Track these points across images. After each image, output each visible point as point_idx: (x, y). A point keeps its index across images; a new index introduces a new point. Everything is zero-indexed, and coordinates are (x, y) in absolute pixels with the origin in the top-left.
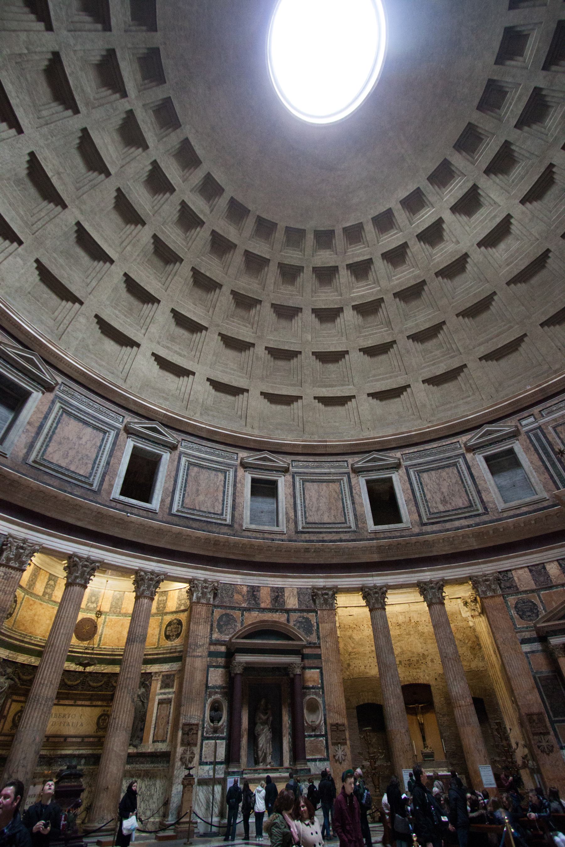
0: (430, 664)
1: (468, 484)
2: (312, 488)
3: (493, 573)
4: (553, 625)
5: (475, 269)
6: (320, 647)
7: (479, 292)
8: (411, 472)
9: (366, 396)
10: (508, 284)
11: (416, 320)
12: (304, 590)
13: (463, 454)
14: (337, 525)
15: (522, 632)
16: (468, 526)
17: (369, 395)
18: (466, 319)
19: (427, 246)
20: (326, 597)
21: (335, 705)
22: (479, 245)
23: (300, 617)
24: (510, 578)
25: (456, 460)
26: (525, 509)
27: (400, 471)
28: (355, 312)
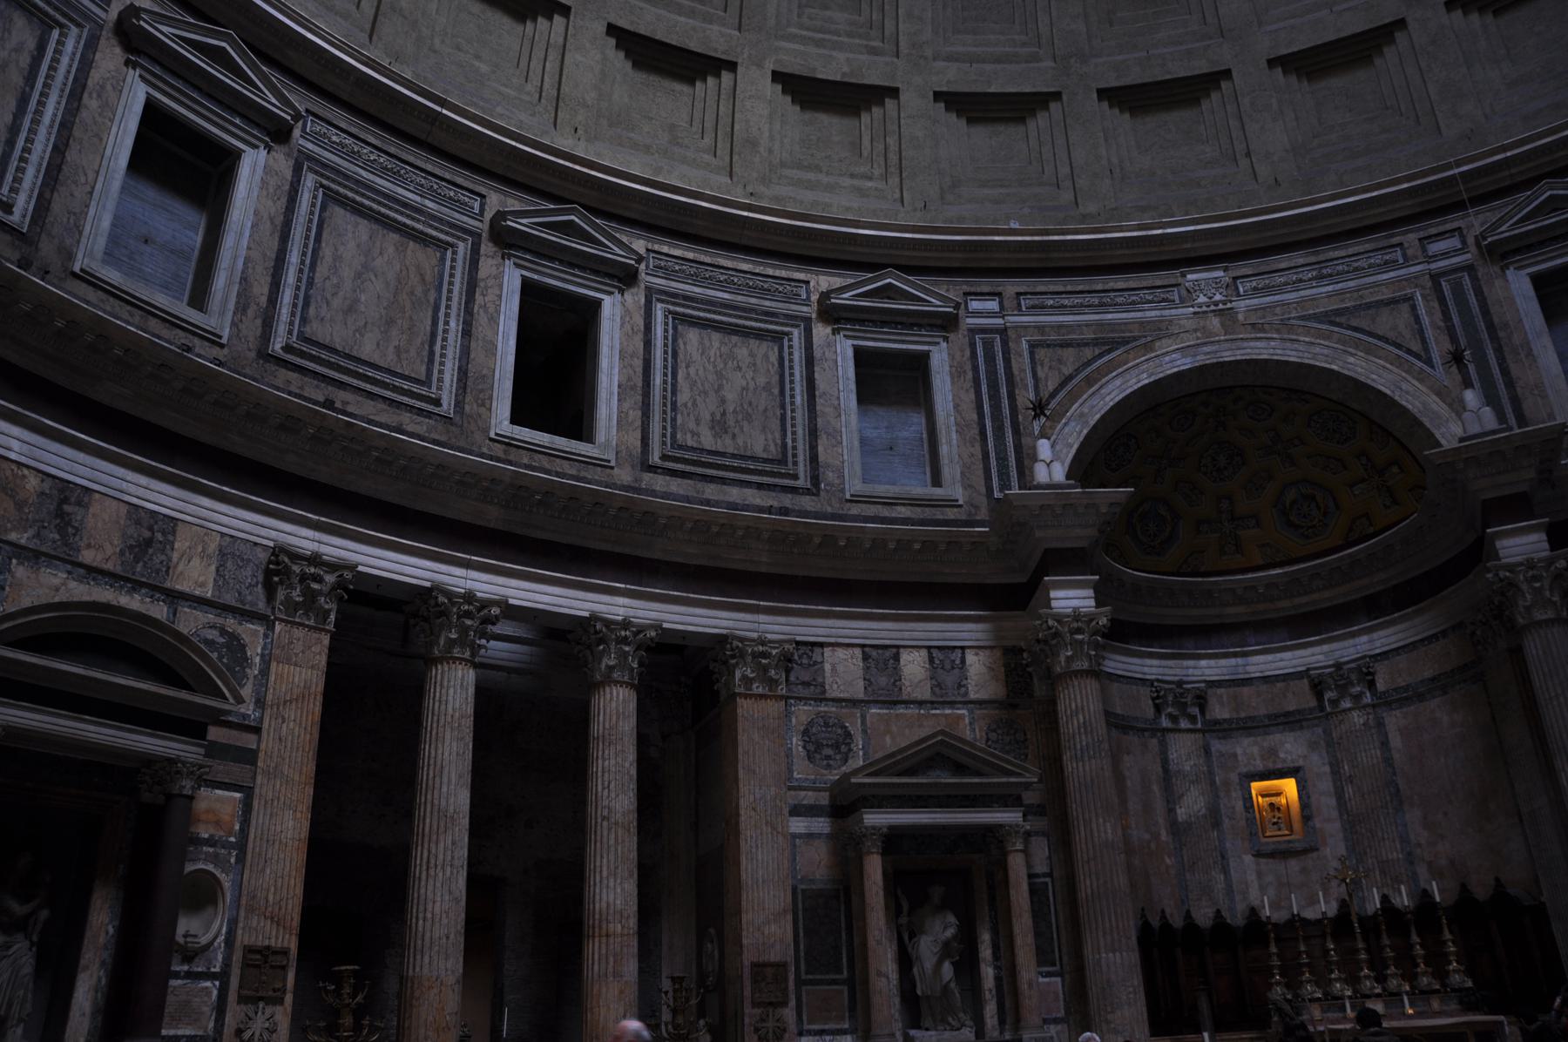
1: (792, 403)
2: (350, 233)
4: (884, 785)
6: (257, 730)
8: (659, 310)
9: (601, 28)
12: (242, 547)
13: (807, 321)
14: (398, 382)
15: (800, 788)
17: (612, 30)
20: (315, 586)
21: (271, 898)
23: (213, 627)
24: (816, 663)
26: (903, 512)
27: (628, 296)
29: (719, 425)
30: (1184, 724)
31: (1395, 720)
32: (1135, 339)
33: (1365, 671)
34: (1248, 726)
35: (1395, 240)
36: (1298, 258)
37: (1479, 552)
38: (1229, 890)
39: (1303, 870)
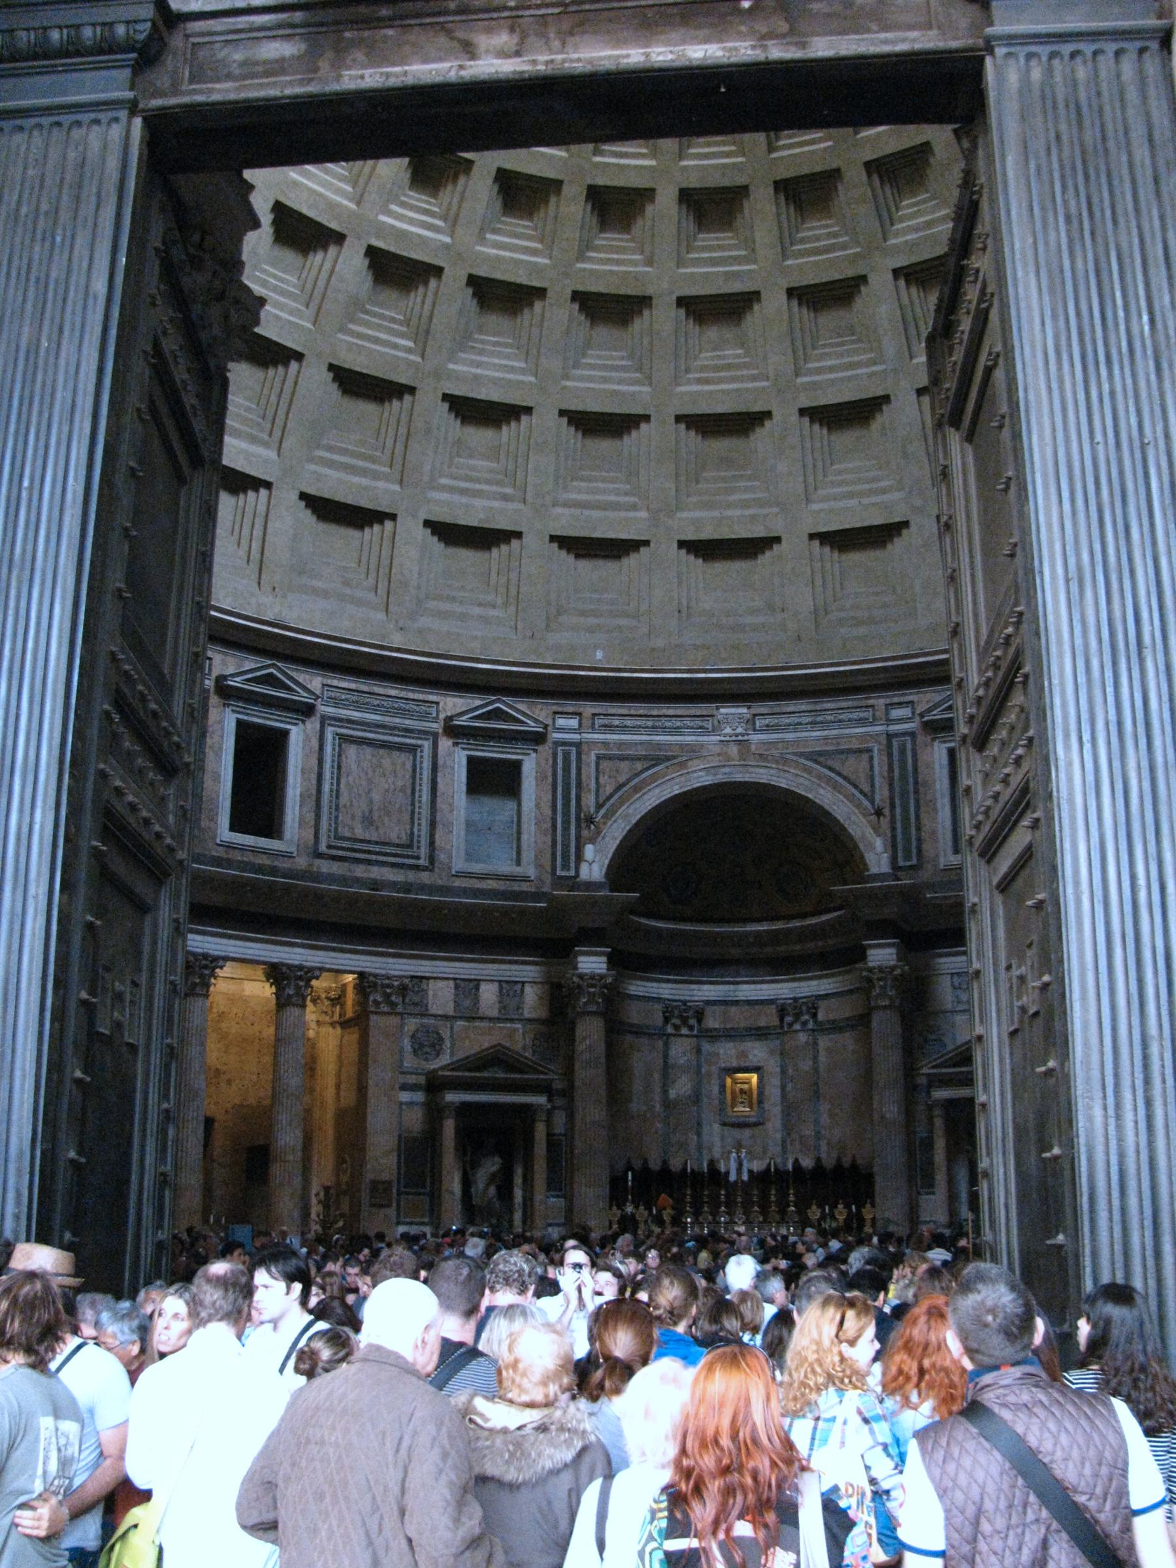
0: (223, 1085)
3: (401, 977)
5: (646, 341)
7: (623, 394)
8: (330, 732)
9: (294, 496)
10: (679, 419)
11: (479, 365)
13: (435, 736)
16: (394, 885)
17: (303, 496)
18: (572, 429)
19: (595, 221)
22: (682, 302)
25: (419, 742)
27: (309, 725)
28: (367, 262)
29: (368, 821)
30: (684, 1031)
31: (824, 1042)
32: (675, 757)
33: (812, 1005)
34: (730, 1035)
35: (871, 702)
36: (802, 705)
37: (859, 954)
38: (700, 1147)
39: (752, 1137)
